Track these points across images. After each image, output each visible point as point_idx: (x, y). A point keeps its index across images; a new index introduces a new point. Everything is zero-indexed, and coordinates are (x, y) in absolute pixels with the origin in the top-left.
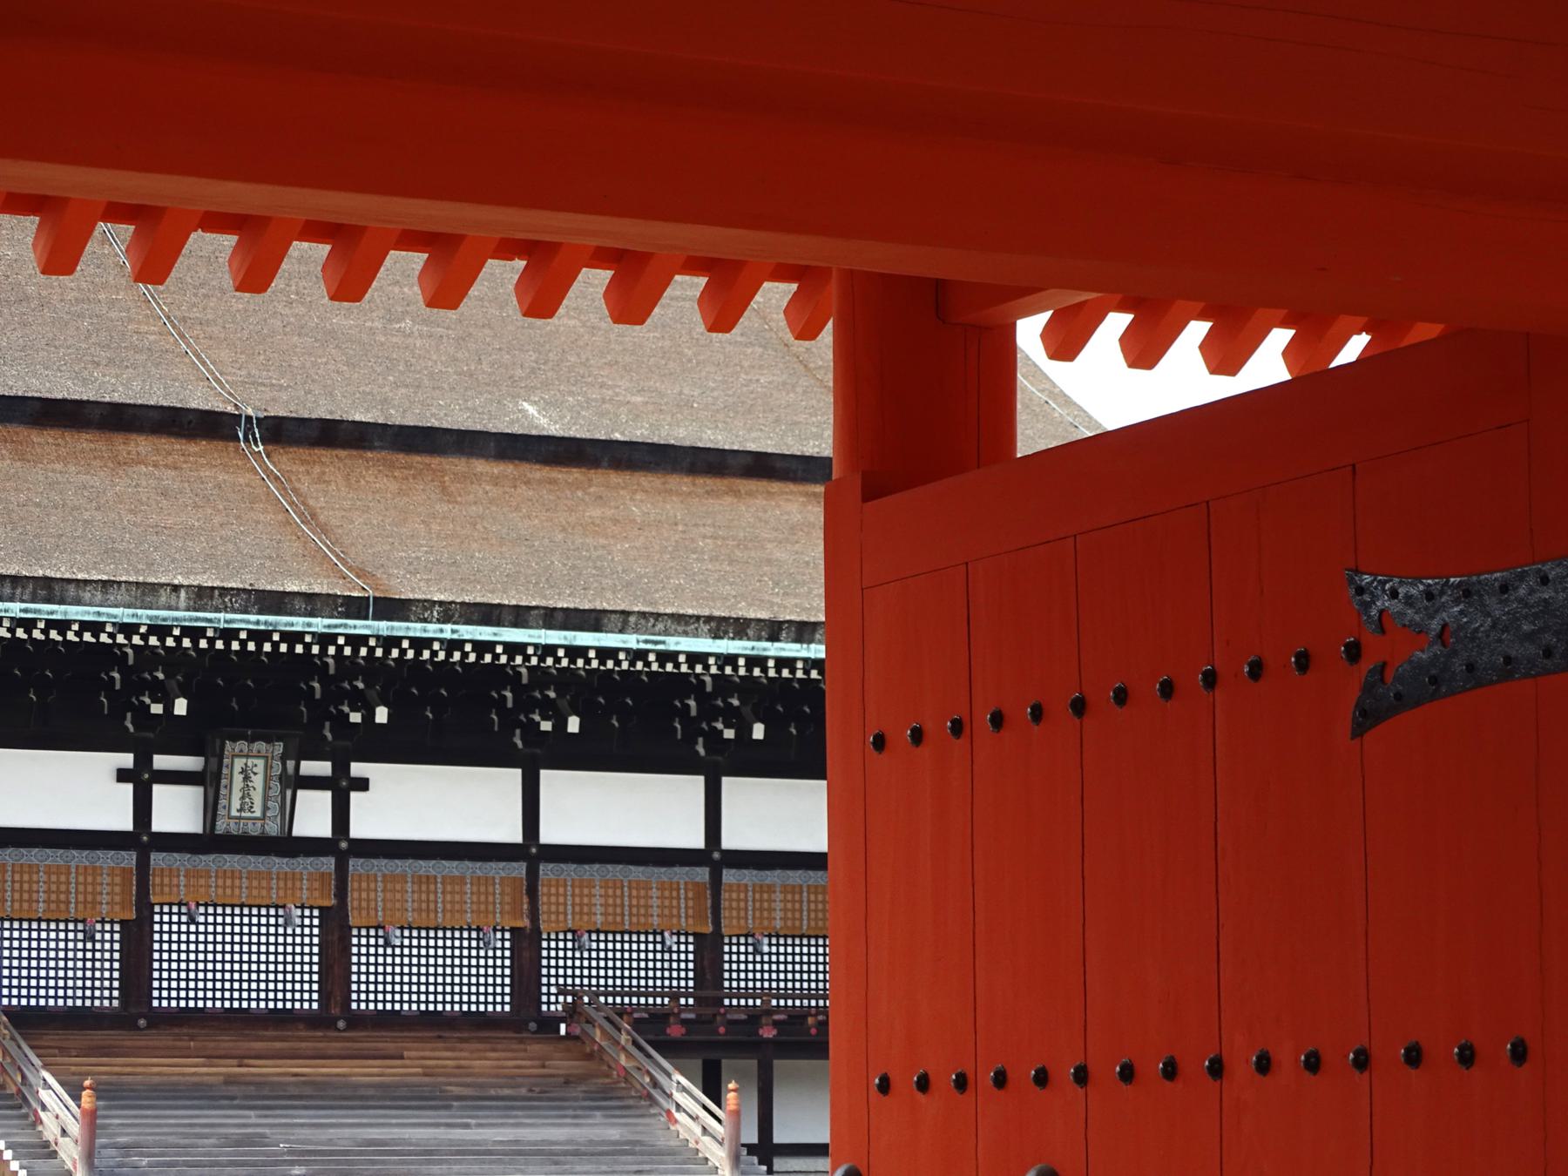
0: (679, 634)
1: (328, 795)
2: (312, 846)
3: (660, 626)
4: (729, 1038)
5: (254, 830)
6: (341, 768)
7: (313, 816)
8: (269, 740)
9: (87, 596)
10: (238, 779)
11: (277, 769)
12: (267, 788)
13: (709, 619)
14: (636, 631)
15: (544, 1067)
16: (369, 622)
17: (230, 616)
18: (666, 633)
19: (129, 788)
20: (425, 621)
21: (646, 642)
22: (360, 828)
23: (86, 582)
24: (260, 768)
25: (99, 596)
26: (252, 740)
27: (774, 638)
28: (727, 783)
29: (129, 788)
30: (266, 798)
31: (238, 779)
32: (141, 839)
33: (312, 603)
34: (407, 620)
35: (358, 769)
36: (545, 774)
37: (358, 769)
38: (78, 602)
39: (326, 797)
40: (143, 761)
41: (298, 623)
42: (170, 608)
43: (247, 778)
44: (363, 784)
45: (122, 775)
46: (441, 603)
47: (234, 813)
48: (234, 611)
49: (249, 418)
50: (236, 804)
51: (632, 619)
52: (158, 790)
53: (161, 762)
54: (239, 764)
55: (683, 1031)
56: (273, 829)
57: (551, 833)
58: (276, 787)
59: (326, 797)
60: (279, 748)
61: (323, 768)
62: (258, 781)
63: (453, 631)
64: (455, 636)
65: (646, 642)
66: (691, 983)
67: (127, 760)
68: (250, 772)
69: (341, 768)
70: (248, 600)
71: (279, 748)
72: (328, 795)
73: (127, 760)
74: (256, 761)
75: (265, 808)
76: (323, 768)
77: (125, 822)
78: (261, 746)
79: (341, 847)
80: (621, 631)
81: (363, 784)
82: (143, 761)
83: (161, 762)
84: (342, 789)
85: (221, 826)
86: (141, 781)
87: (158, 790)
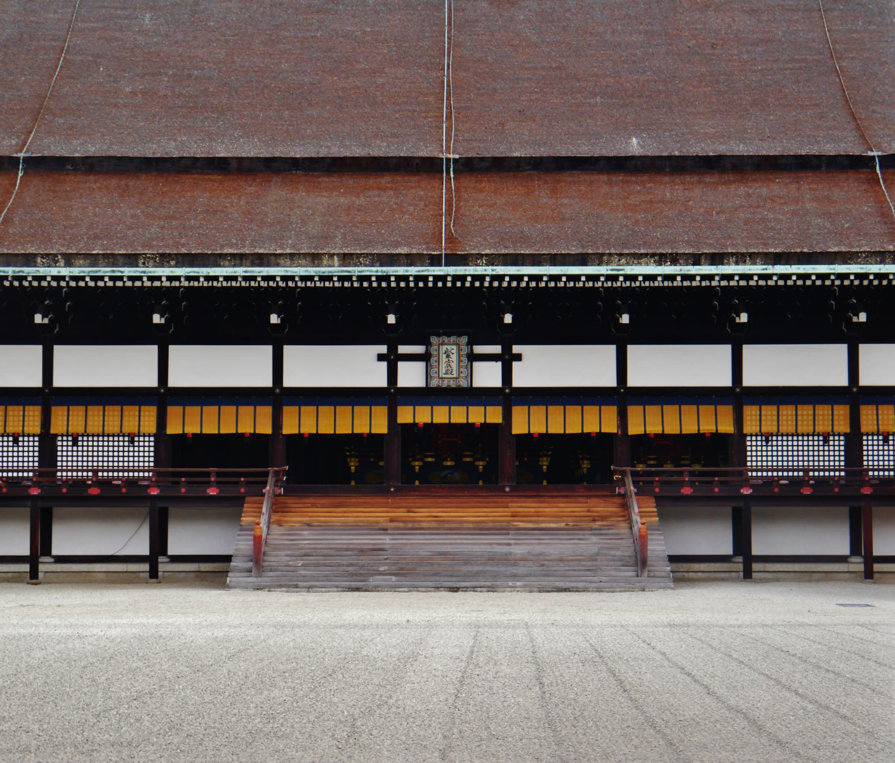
0: (636, 265)
1: (499, 364)
3: (623, 261)
4: (720, 494)
5: (453, 384)
6: (507, 349)
7: (488, 376)
8: (459, 335)
9: (282, 262)
11: (465, 350)
12: (460, 361)
13: (653, 255)
14: (607, 264)
15: (589, 511)
16: (443, 268)
17: (360, 269)
18: (628, 264)
19: (384, 365)
20: (477, 265)
21: (612, 270)
22: (518, 382)
23: (280, 255)
24: (454, 351)
25: (288, 262)
26: (449, 335)
27: (697, 263)
28: (746, 348)
29: (384, 365)
30: (459, 367)
31: (443, 358)
33: (411, 260)
34: (467, 265)
35: (516, 349)
36: (630, 348)
38: (278, 265)
39: (498, 366)
40: (392, 349)
41: (401, 270)
42: (330, 266)
43: (448, 356)
44: (518, 357)
45: (381, 358)
46: (486, 255)
48: (366, 266)
49: (448, 160)
50: (443, 370)
51: (605, 258)
52: (402, 366)
53: (403, 349)
54: (444, 348)
55: (692, 490)
56: (464, 383)
57: (634, 380)
58: (465, 360)
59: (498, 366)
60: (464, 339)
61: (496, 349)
62: (454, 357)
63: (493, 270)
64: (494, 273)
65: (612, 270)
66: (842, 463)
67: (383, 349)
68: (449, 355)
69: (507, 349)
70: (373, 259)
71: (464, 339)
72: (499, 364)
73: (383, 349)
75: (460, 372)
76: (496, 349)
77: (381, 382)
78: (452, 339)
80: (599, 265)
81: (518, 357)
82: (392, 349)
83: (403, 349)
84: (508, 360)
85: (434, 383)
86: (392, 360)
87: (402, 366)
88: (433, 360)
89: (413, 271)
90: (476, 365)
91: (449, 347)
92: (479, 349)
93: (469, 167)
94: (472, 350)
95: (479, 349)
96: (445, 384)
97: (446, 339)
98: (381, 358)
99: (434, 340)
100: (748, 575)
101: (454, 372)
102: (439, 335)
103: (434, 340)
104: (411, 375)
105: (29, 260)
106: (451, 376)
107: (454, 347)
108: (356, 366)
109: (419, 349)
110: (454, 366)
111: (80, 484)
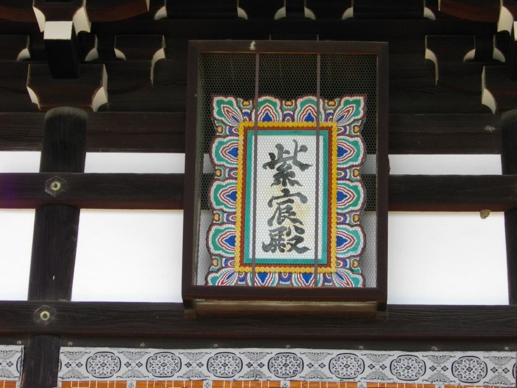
8: (331, 93)
10: (265, 178)
12: (330, 196)
26: (288, 93)
31: (265, 184)
43: (283, 177)
47: (261, 255)
50: (263, 235)
52: (95, 227)
53: (98, 162)
54: (266, 145)
60: (352, 109)
62: (307, 182)
71: (352, 109)
74: (303, 140)
78: (305, 105)
87: (95, 227)
88: (217, 192)
90: (402, 224)
91: (288, 141)
92: (406, 164)
94: (384, 165)
95: (406, 164)
97: (270, 105)
101: (308, 241)
102: (246, 93)
103: (227, 110)
106: (294, 255)
107: (309, 141)
109: (169, 163)
110: (308, 214)
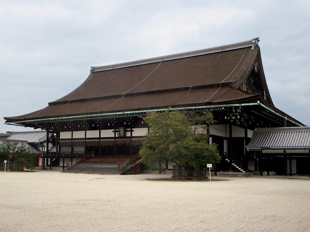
2: (129, 137)
6: (131, 129)
7: (128, 134)
32: (115, 138)
35: (133, 129)
37: (133, 129)
40: (115, 130)
44: (133, 131)
45: (113, 132)
61: (130, 129)
62: (123, 131)
67: (114, 130)
73: (114, 130)
76: (130, 129)
79: (132, 137)
81: (133, 131)
84: (132, 131)
86: (115, 132)
89: (95, 115)
93: (127, 96)
96: (121, 136)
98: (113, 132)
99: (119, 128)
100: (160, 173)
103: (119, 128)
104: (117, 136)
105: (50, 117)
108: (108, 133)
111: (76, 154)
